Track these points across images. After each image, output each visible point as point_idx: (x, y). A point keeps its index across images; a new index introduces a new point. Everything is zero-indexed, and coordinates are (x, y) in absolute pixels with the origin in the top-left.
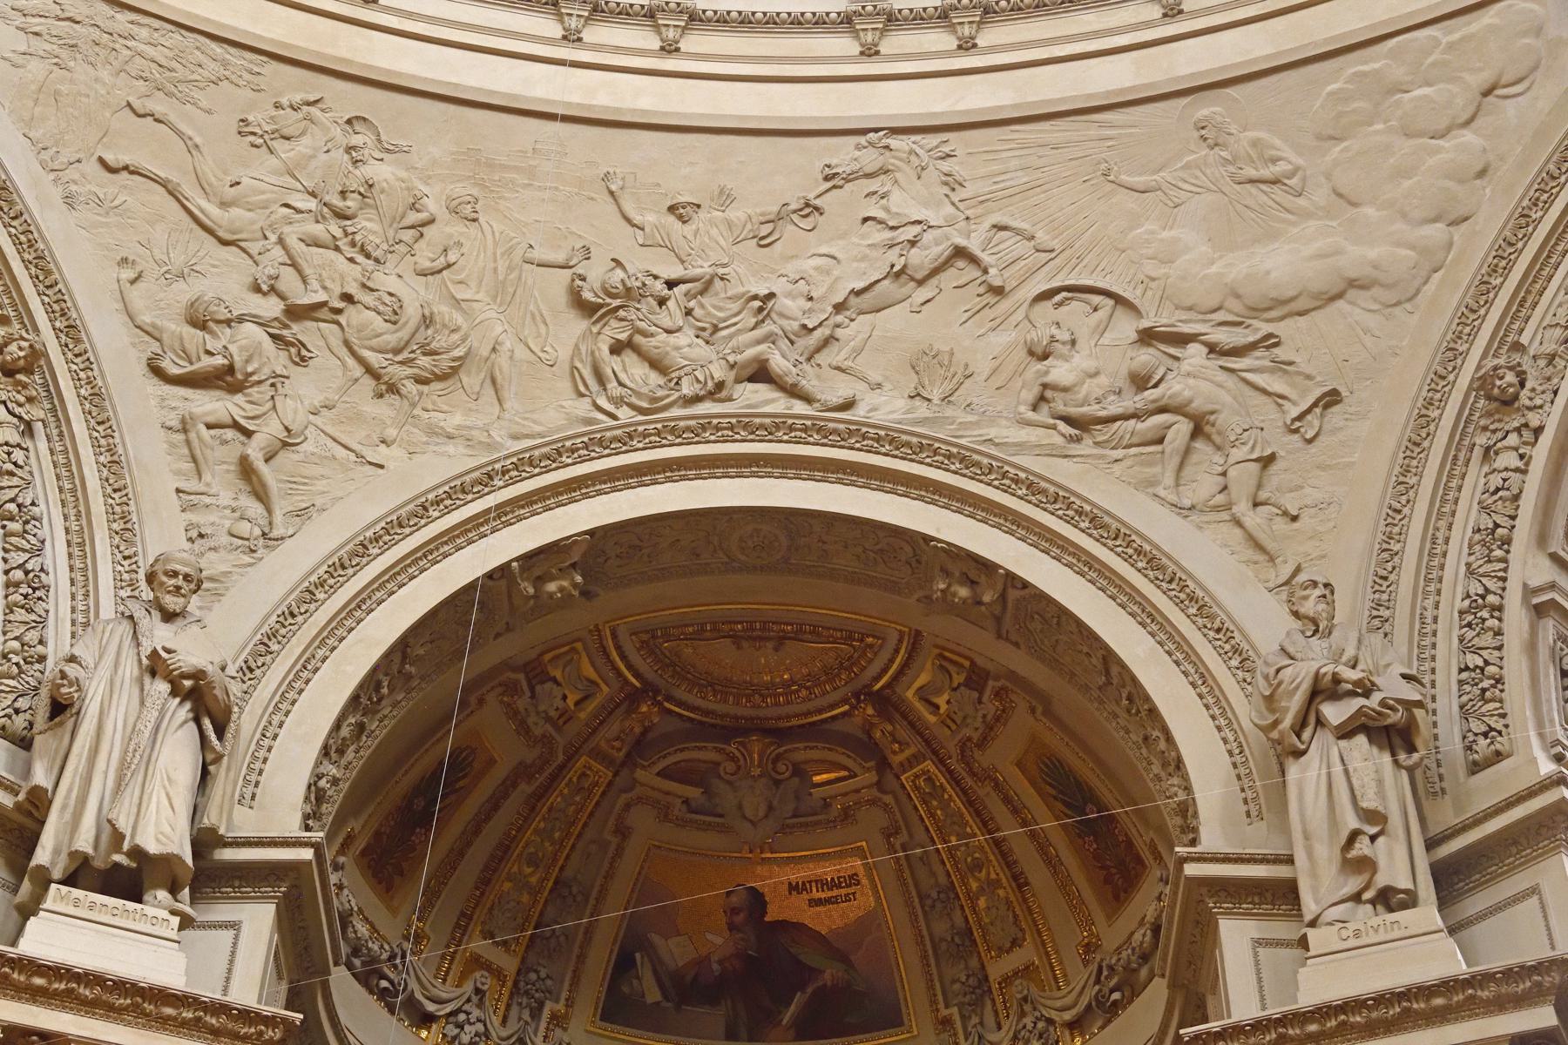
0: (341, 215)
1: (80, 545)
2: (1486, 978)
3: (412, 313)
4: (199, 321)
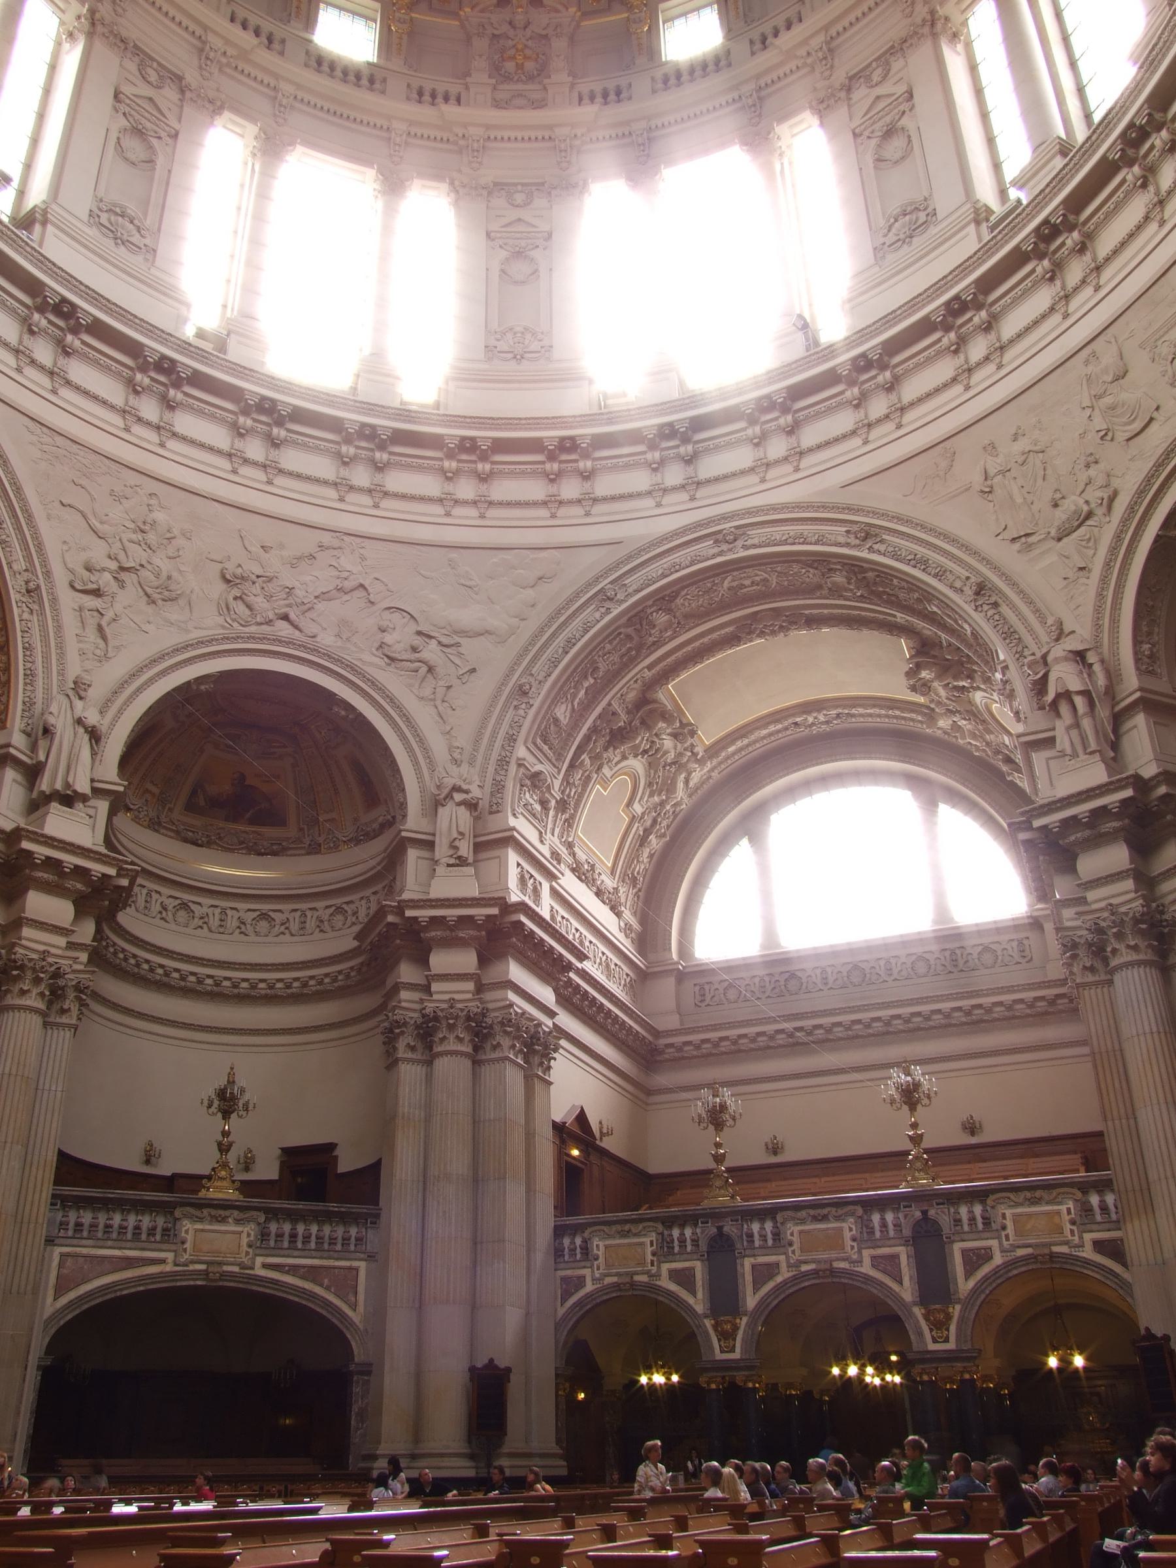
0: (143, 532)
1: (46, 658)
2: (484, 899)
3: (164, 575)
4: (89, 569)
